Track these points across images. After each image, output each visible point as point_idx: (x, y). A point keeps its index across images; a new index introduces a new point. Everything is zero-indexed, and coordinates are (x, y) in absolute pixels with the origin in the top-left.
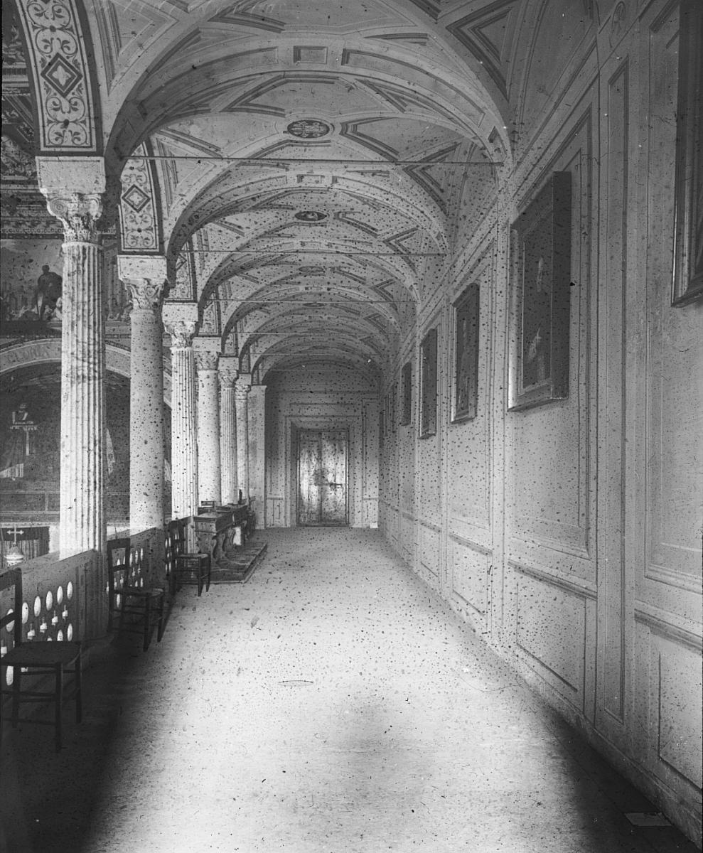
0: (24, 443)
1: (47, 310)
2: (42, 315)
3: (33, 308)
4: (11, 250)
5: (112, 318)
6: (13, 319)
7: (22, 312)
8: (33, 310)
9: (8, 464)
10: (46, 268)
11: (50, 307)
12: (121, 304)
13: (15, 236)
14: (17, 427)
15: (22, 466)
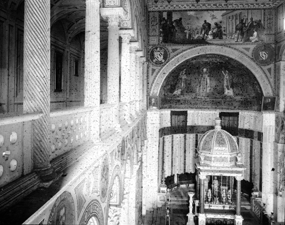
0: (182, 82)
1: (206, 35)
2: (204, 37)
3: (201, 34)
4: (194, 15)
5: (228, 38)
6: (194, 39)
7: (197, 36)
8: (201, 36)
9: (177, 89)
10: (205, 21)
11: (207, 34)
12: (232, 33)
13: (194, 10)
14: (181, 77)
15: (180, 90)
